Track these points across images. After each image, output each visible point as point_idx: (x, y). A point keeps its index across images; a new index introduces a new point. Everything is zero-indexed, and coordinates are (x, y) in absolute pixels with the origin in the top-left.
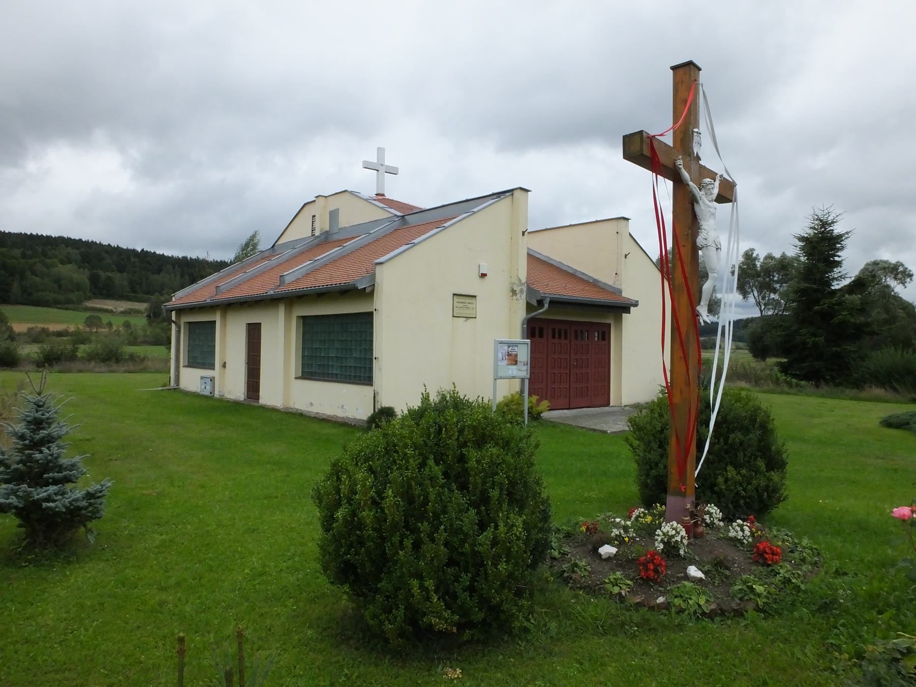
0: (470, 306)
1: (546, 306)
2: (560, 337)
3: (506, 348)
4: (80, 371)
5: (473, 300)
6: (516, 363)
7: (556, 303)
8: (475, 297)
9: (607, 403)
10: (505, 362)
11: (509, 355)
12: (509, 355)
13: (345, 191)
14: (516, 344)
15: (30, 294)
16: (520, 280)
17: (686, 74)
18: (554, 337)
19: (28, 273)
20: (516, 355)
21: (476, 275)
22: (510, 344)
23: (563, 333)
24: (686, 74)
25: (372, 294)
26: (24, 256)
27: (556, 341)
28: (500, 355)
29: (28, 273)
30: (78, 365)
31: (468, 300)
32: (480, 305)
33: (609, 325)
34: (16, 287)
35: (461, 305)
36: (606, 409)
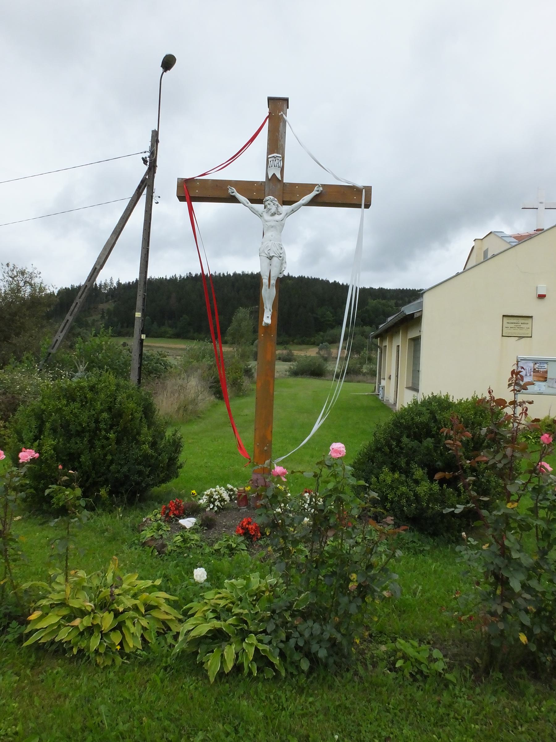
0: (522, 326)
3: (531, 365)
4: (359, 382)
5: (529, 321)
6: (545, 379)
8: (531, 317)
13: (491, 233)
14: (546, 362)
17: (278, 105)
20: (546, 372)
21: (535, 296)
22: (536, 362)
24: (278, 105)
25: (420, 318)
30: (360, 377)
31: (521, 321)
32: (538, 327)
35: (513, 325)
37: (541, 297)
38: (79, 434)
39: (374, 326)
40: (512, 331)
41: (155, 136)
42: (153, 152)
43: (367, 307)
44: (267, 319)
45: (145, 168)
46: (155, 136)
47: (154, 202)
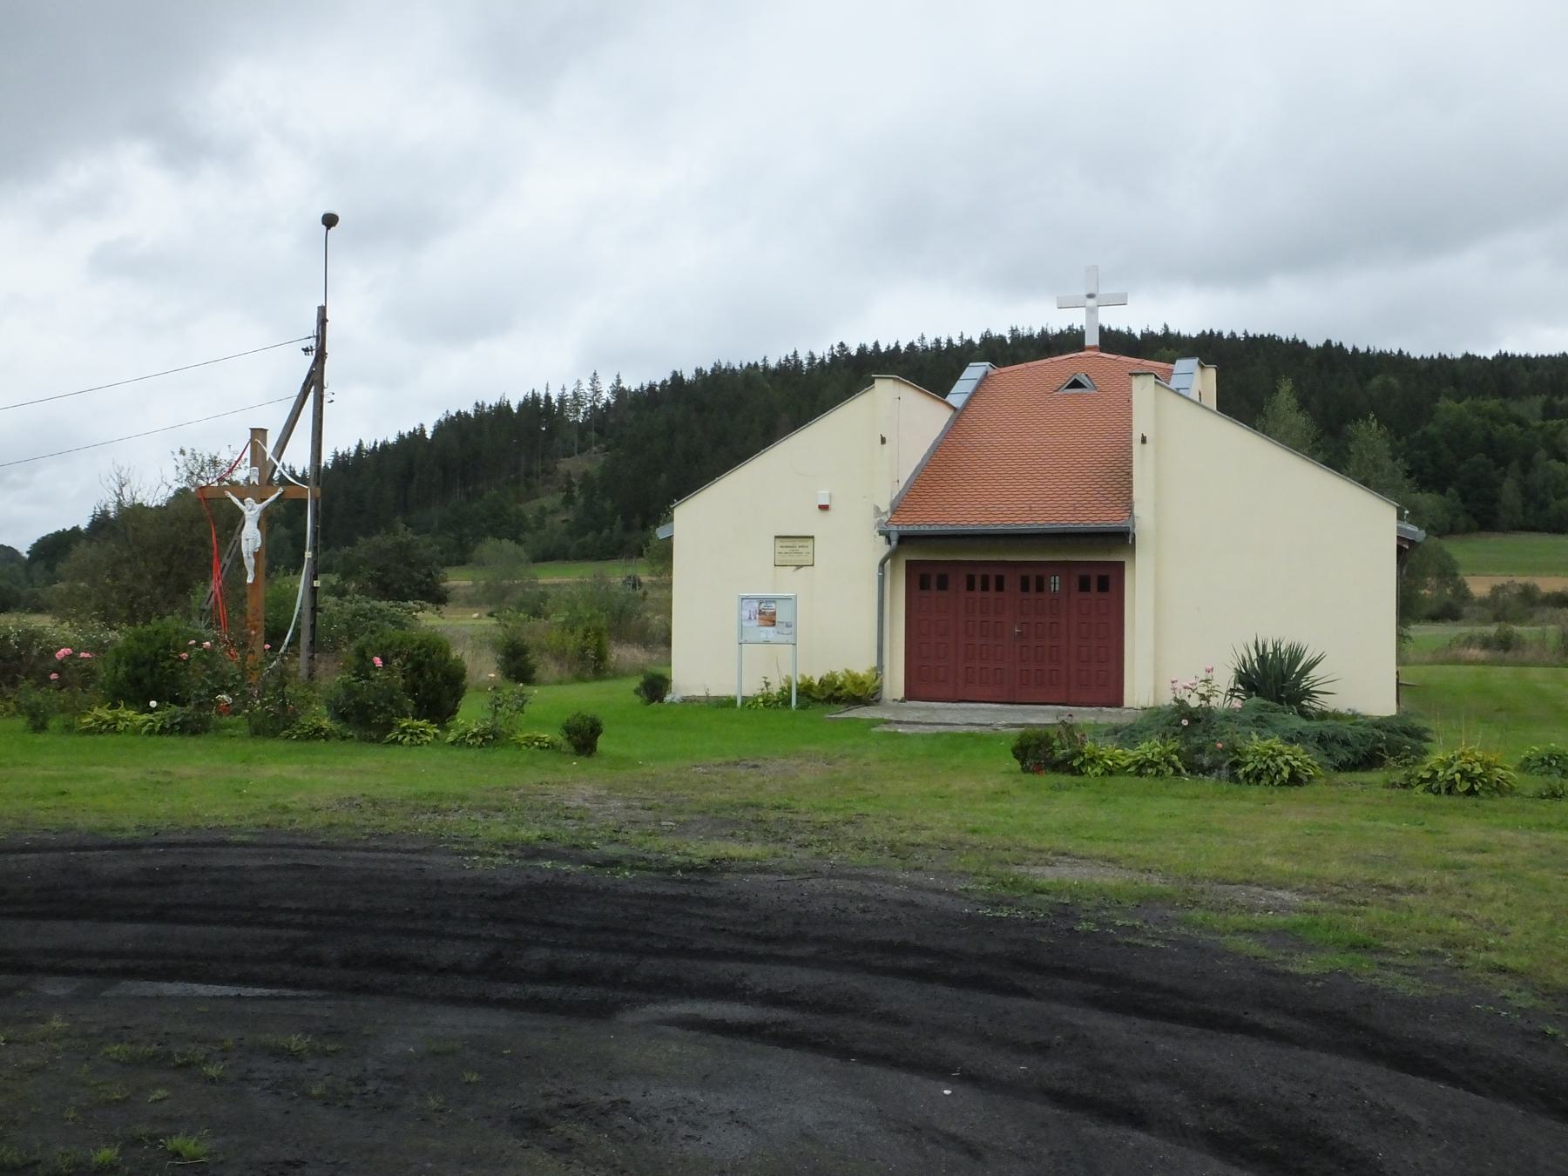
1: (894, 543)
2: (985, 588)
7: (906, 540)
9: (1117, 702)
10: (756, 623)
11: (761, 613)
12: (761, 613)
14: (773, 600)
15: (1543, 505)
16: (877, 509)
18: (971, 587)
19: (1542, 454)
22: (761, 601)
23: (934, 580)
26: (1549, 412)
27: (978, 593)
28: (746, 614)
29: (1542, 454)
31: (798, 543)
33: (1120, 567)
34: (1509, 491)
37: (824, 508)
38: (144, 665)
39: (1451, 490)
40: (787, 557)
41: (322, 311)
42: (321, 337)
43: (1432, 429)
44: (250, 580)
45: (311, 358)
46: (322, 311)
47: (326, 400)
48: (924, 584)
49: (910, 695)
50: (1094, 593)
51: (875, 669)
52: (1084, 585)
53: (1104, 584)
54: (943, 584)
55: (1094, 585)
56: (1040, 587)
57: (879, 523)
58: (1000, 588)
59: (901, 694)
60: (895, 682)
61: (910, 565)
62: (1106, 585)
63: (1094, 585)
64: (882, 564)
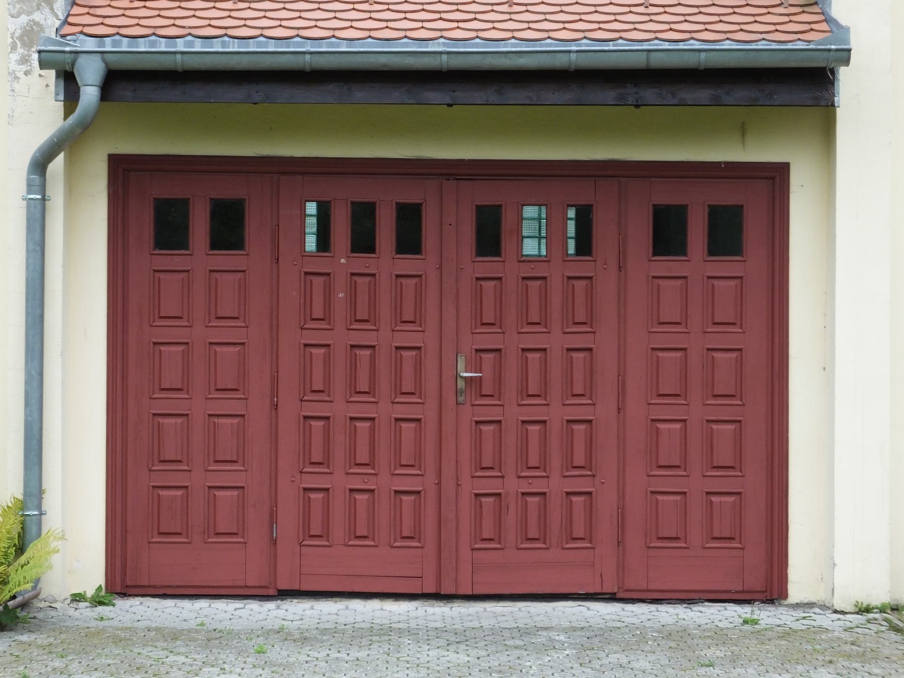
1: (90, 94)
2: (364, 243)
7: (121, 80)
9: (771, 589)
33: (776, 178)
36: (766, 615)
48: (170, 231)
49: (123, 581)
50: (386, 261)
51: (23, 505)
52: (667, 235)
53: (726, 234)
54: (228, 230)
55: (697, 233)
56: (490, 236)
57: (29, 35)
58: (409, 241)
59: (92, 573)
60: (76, 546)
61: (122, 170)
62: (733, 229)
63: (697, 233)
64: (40, 165)
